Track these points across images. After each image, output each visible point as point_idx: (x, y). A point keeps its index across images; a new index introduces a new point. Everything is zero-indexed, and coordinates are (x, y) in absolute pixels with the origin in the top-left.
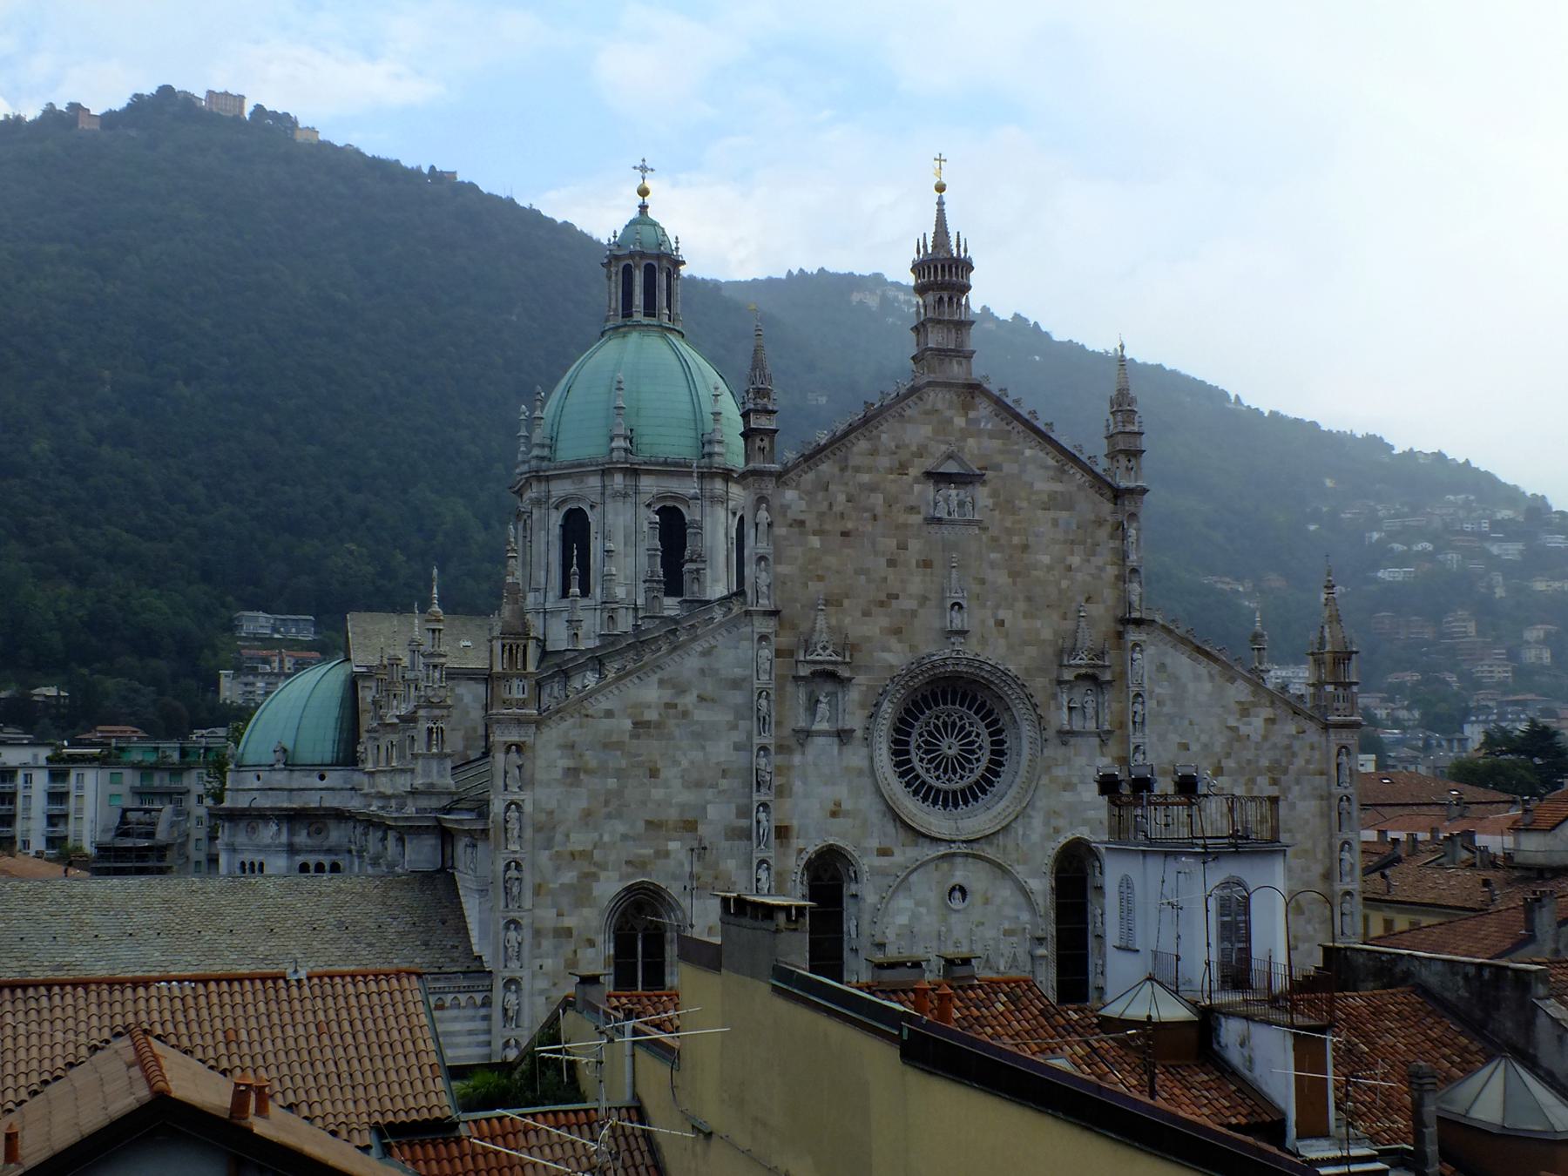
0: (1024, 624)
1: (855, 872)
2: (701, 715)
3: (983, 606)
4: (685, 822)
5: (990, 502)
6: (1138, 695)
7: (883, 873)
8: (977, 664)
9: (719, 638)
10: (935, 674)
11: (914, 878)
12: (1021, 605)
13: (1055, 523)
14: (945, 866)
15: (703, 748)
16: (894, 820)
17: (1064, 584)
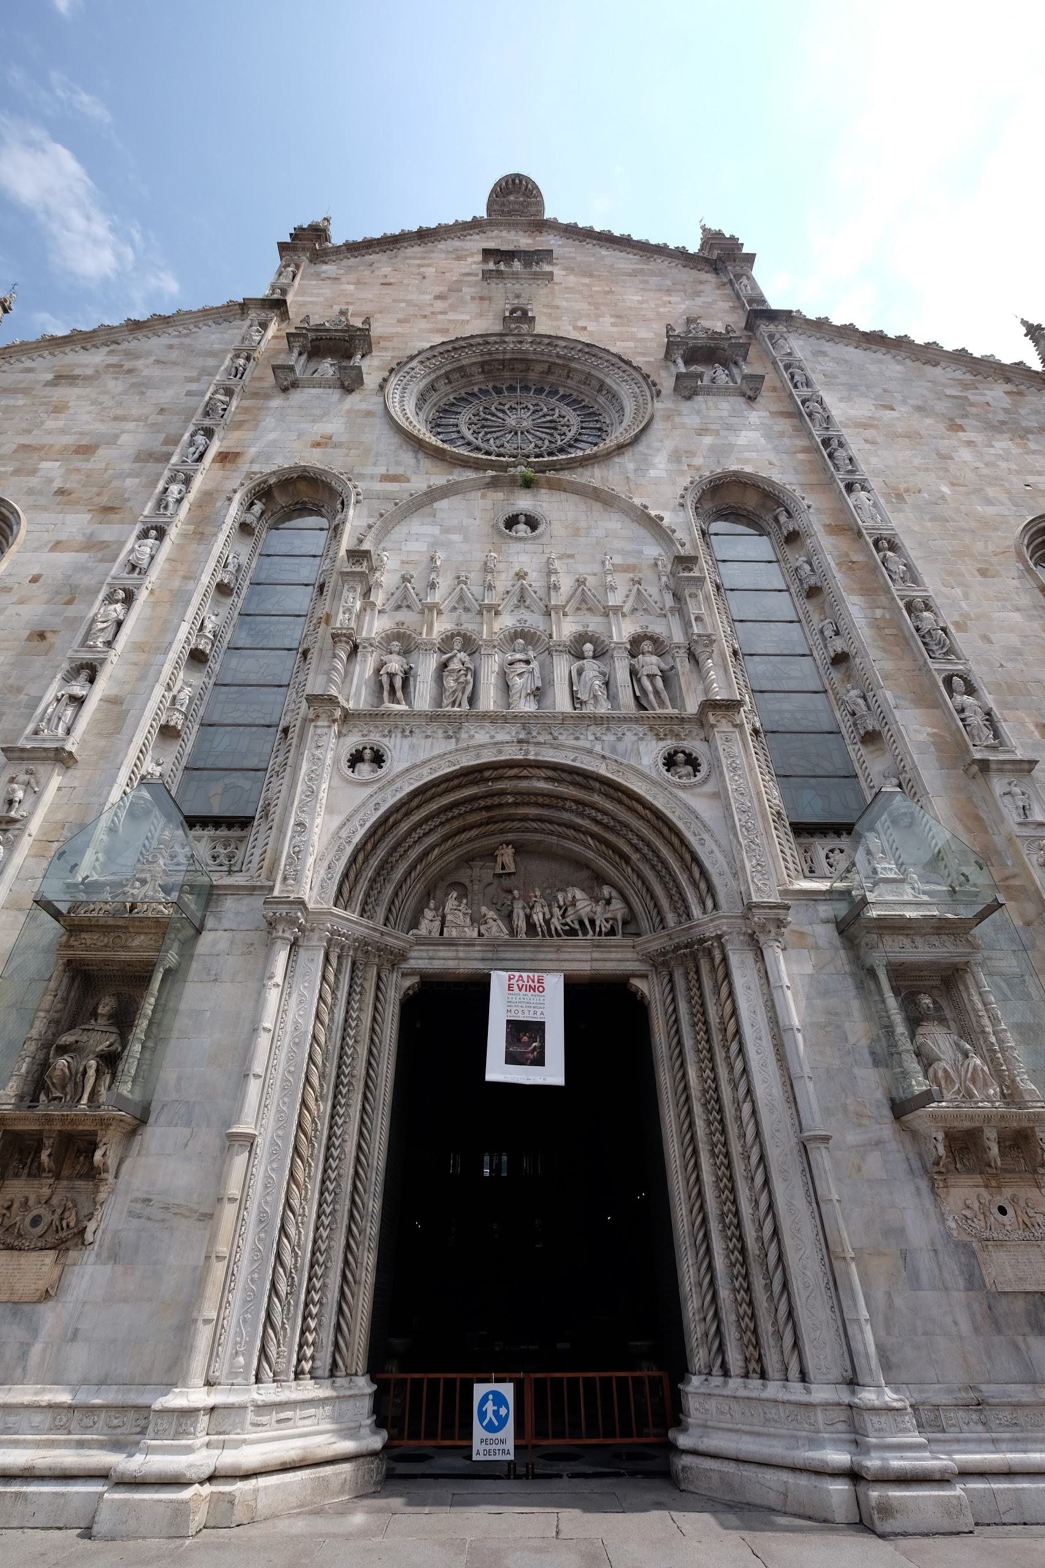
0: (614, 329)
1: (343, 503)
2: (156, 372)
3: (558, 319)
4: (80, 446)
5: (564, 273)
6: (787, 367)
7: (386, 497)
8: (546, 341)
9: (205, 328)
10: (490, 353)
11: (443, 504)
12: (608, 320)
13: (647, 282)
14: (500, 495)
15: (143, 393)
16: (416, 452)
17: (661, 310)
